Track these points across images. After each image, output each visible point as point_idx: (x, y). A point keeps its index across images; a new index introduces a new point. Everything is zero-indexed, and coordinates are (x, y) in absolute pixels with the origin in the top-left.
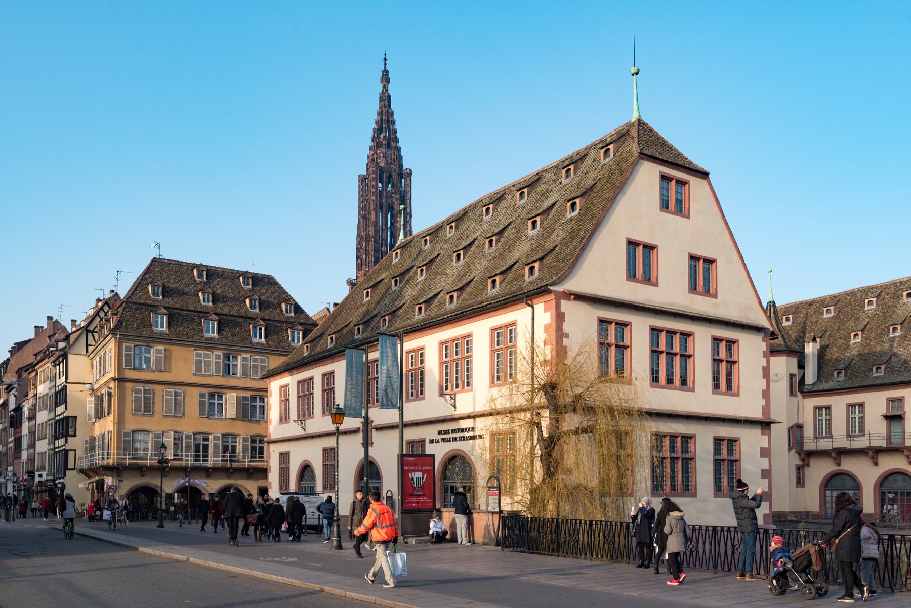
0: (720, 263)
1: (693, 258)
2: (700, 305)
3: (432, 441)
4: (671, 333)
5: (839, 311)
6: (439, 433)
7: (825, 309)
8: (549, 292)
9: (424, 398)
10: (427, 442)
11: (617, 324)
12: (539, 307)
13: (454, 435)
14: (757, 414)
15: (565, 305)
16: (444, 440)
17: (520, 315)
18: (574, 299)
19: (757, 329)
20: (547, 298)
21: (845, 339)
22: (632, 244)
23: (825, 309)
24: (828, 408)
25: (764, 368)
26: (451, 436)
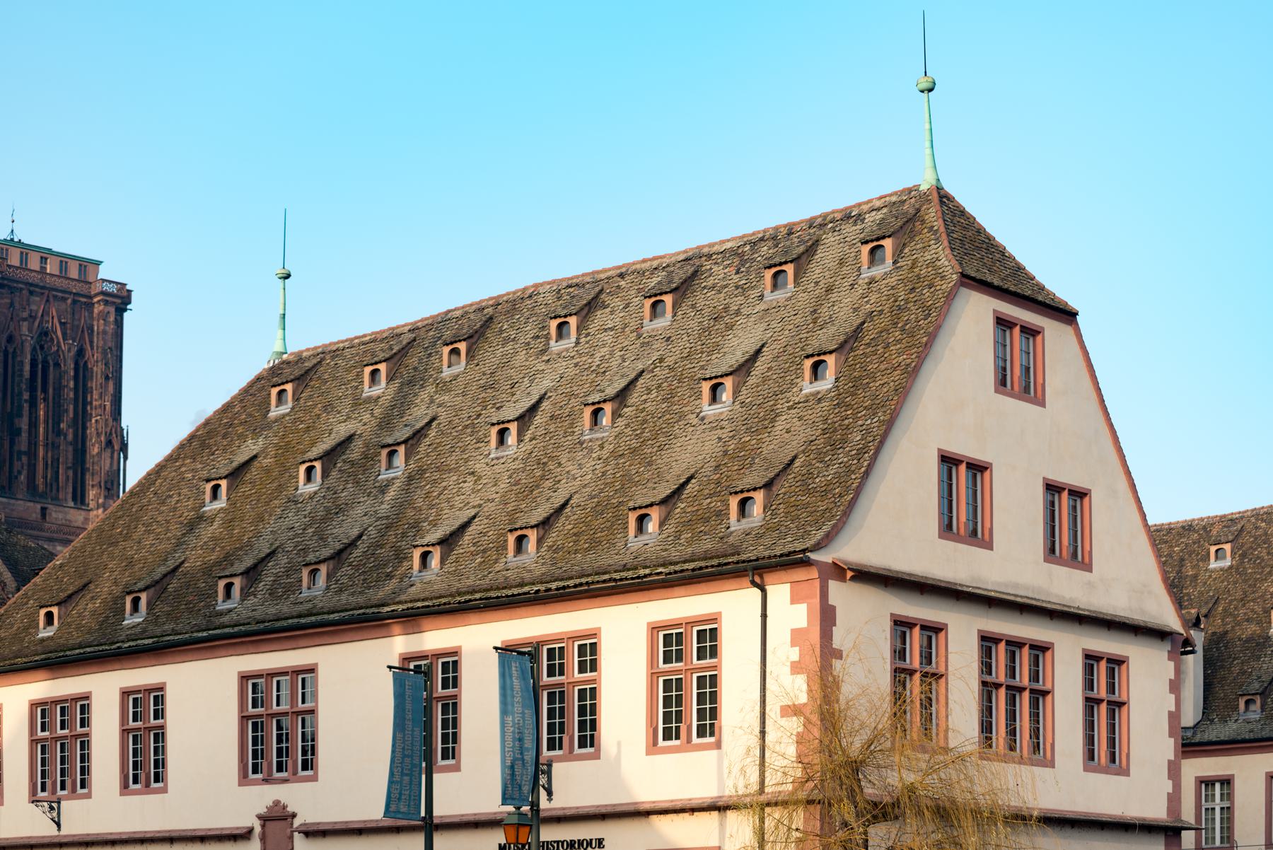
0: (1097, 498)
1: (1052, 488)
2: (1064, 586)
4: (1014, 645)
5: (1243, 556)
7: (1213, 549)
8: (806, 563)
11: (924, 628)
12: (779, 592)
14: (1157, 811)
15: (839, 592)
17: (733, 607)
18: (852, 578)
19: (1158, 634)
20: (800, 574)
21: (1259, 623)
22: (948, 461)
23: (1213, 549)
24: (1227, 782)
25: (1170, 713)
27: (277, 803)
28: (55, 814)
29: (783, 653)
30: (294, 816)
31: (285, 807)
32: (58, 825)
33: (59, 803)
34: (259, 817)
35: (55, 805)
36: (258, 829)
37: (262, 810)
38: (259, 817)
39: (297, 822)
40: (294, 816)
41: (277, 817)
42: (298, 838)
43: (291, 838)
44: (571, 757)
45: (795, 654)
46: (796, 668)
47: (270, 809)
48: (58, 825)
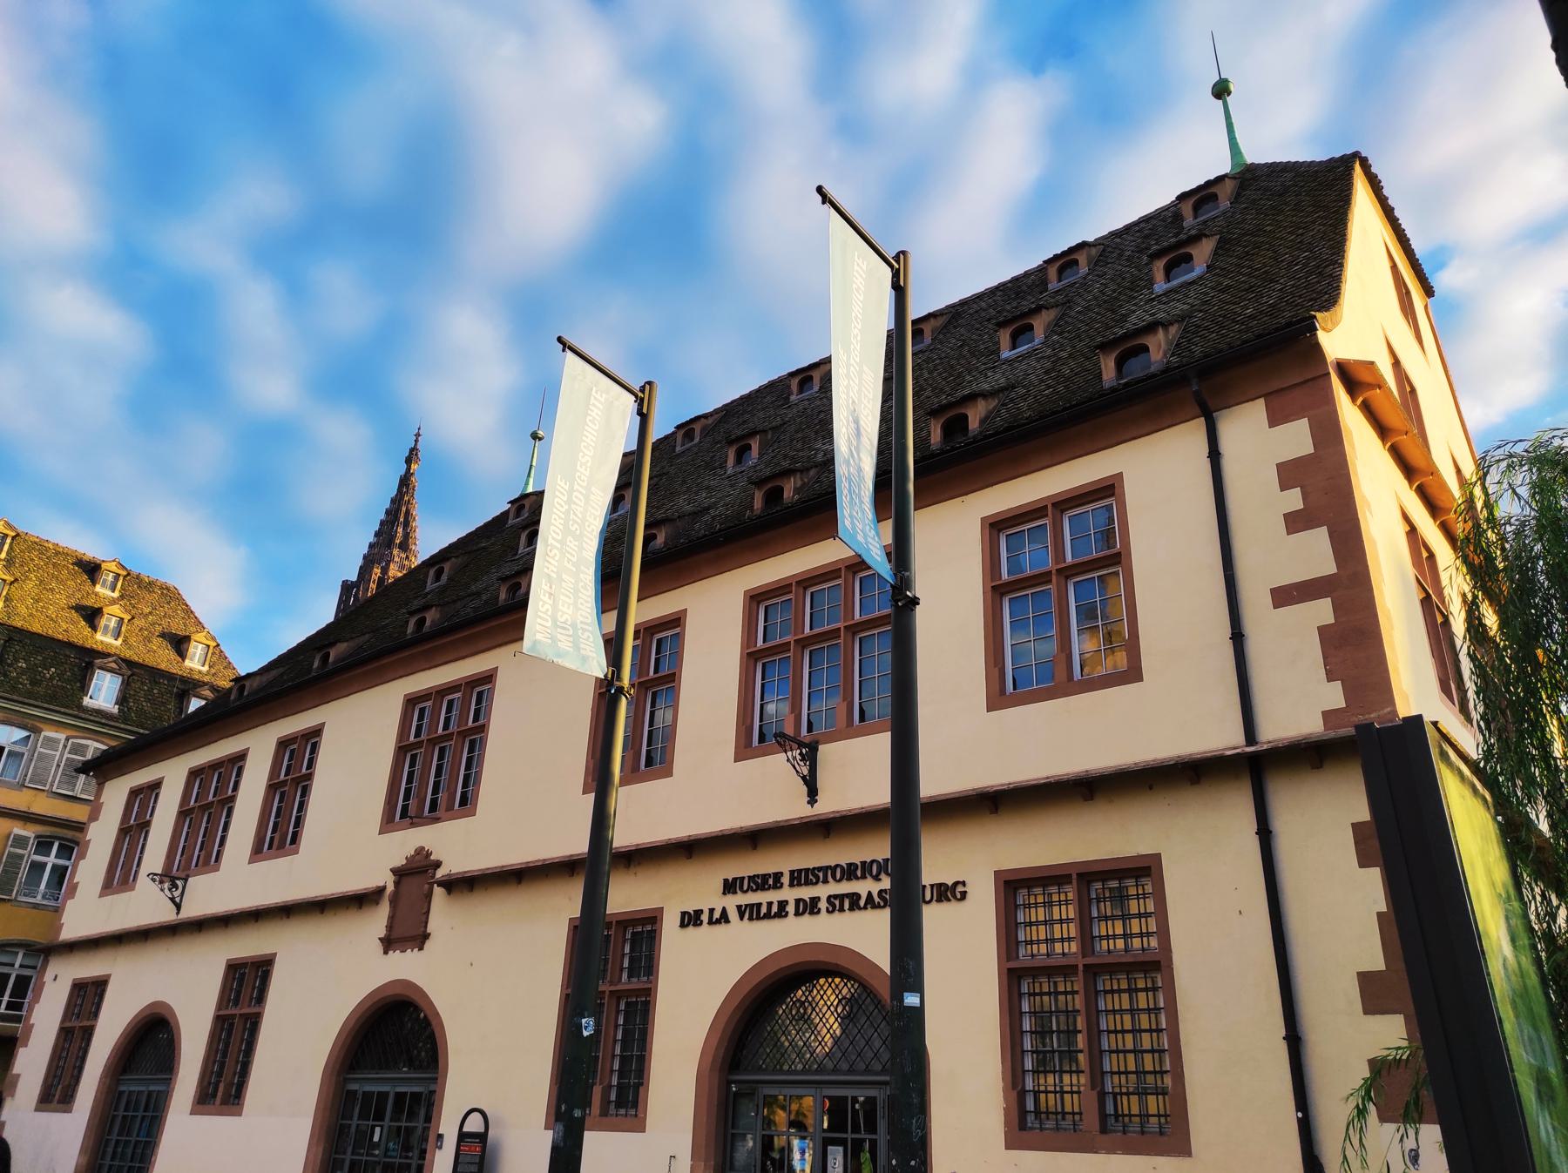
3: (691, 919)
6: (730, 887)
9: (669, 773)
10: (670, 922)
13: (806, 893)
16: (751, 913)
26: (789, 894)
27: (420, 851)
28: (177, 894)
29: (1261, 502)
30: (438, 864)
31: (429, 854)
32: (178, 907)
33: (186, 880)
34: (394, 871)
35: (179, 883)
36: (390, 888)
37: (400, 861)
38: (394, 871)
39: (440, 873)
40: (438, 864)
41: (418, 873)
42: (438, 891)
43: (429, 896)
44: (849, 732)
45: (1294, 500)
46: (1295, 523)
47: (409, 860)
48: (178, 907)
